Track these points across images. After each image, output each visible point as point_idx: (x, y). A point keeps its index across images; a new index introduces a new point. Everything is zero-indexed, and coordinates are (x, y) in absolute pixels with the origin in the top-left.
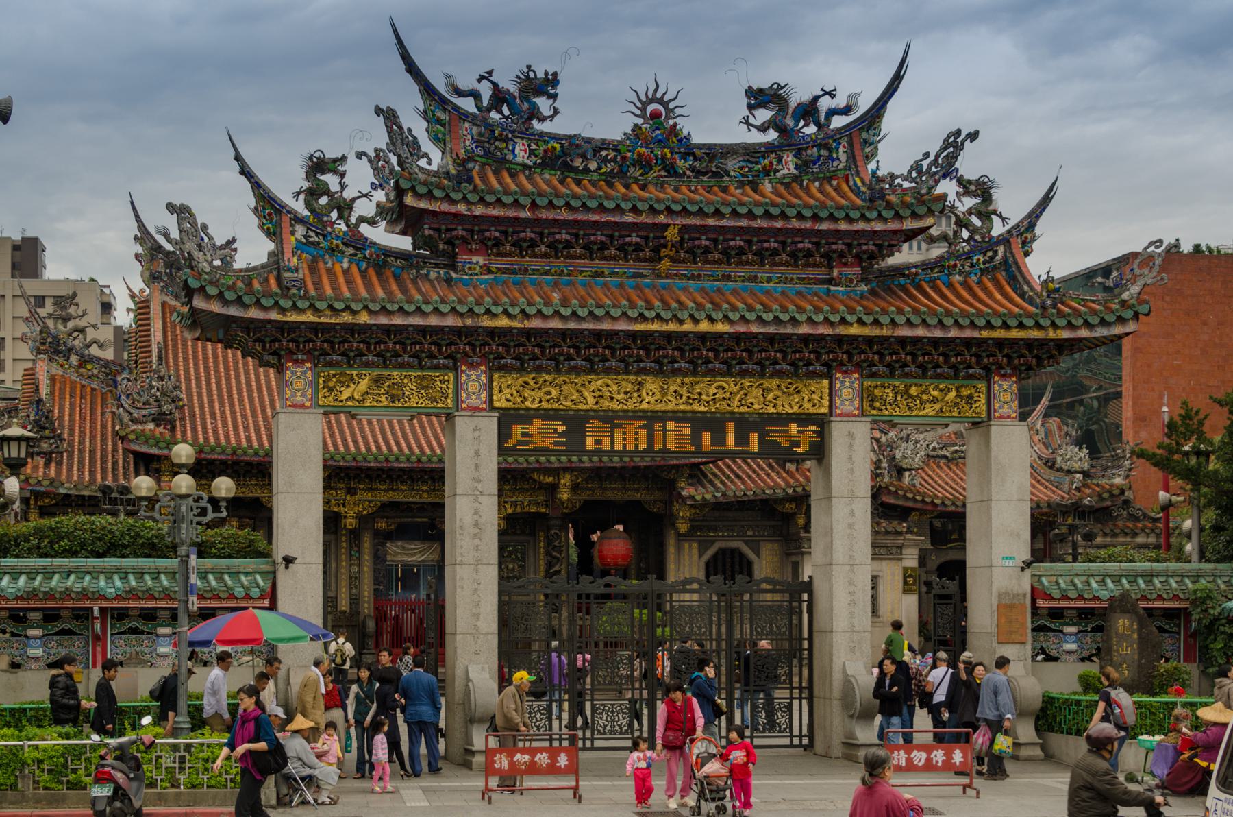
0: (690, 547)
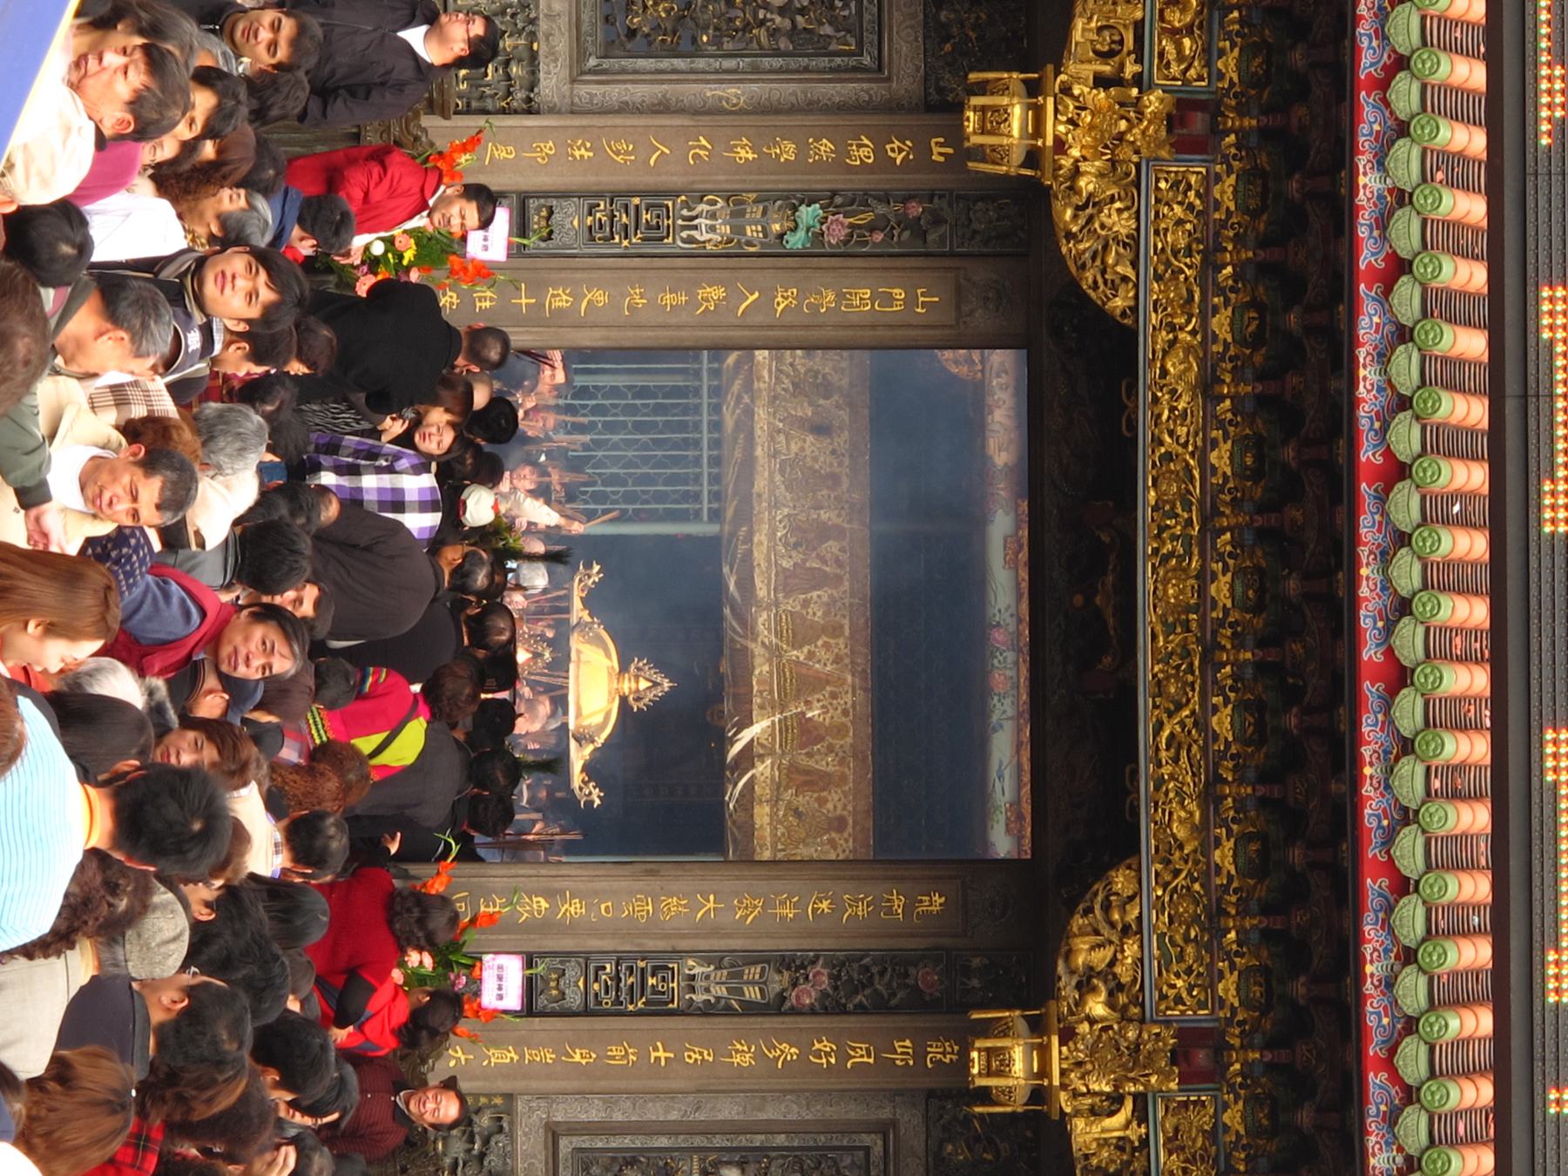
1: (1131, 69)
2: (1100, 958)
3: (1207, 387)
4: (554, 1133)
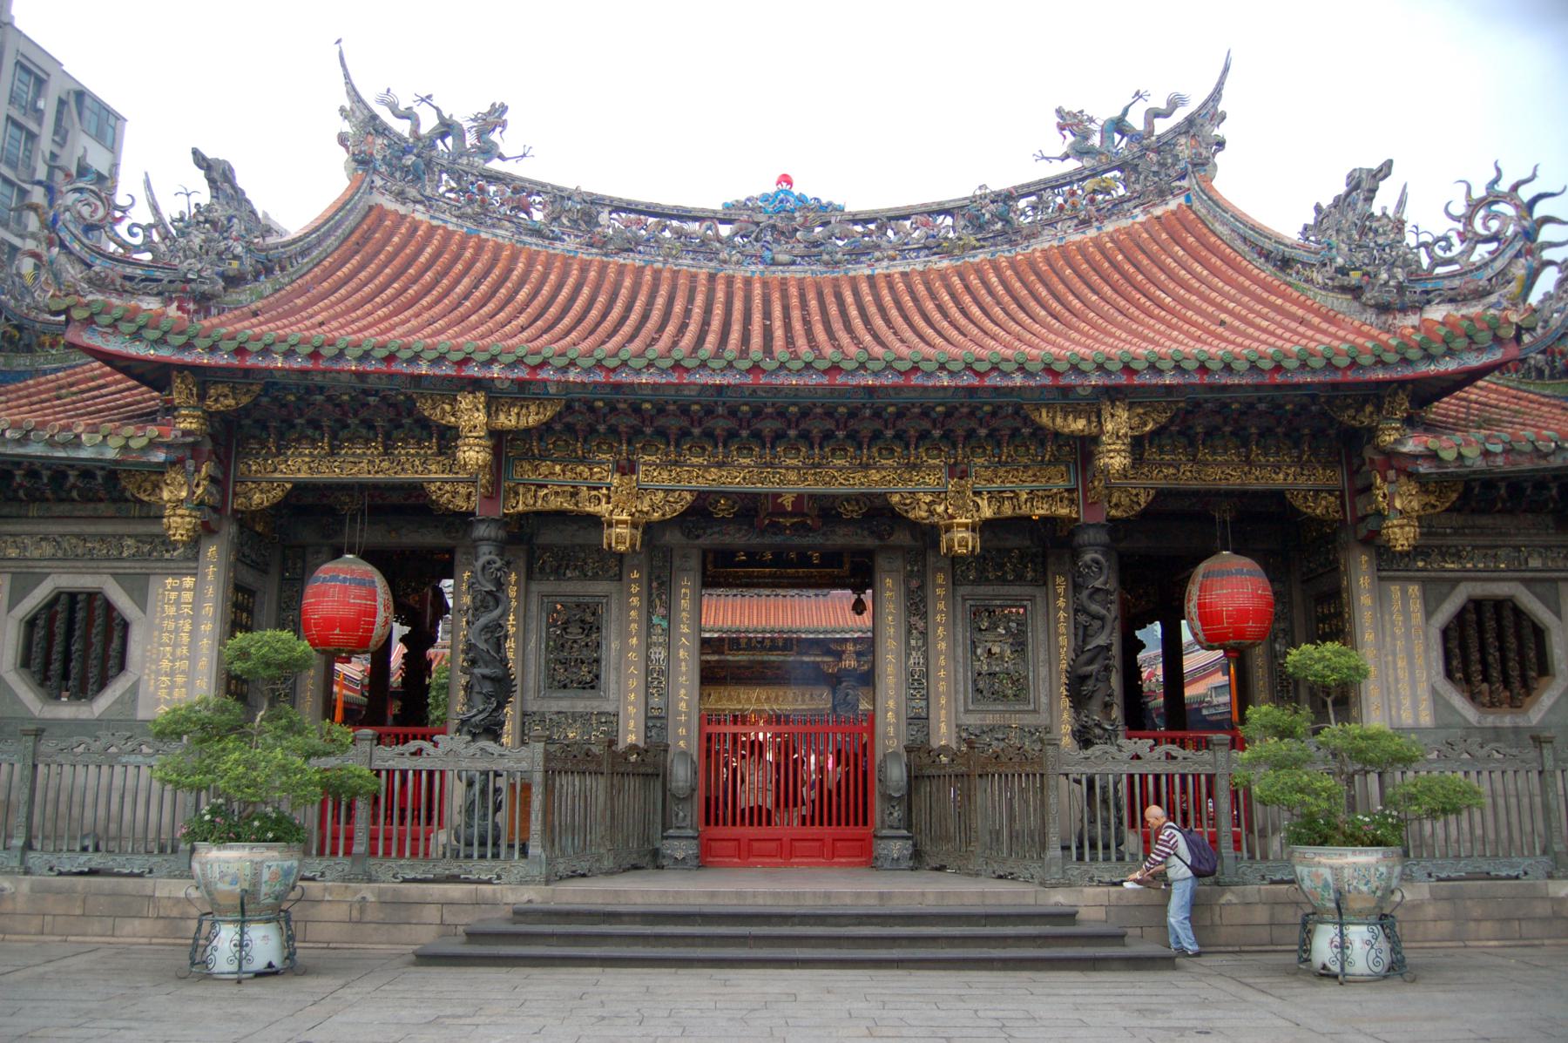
0: (1404, 592)
1: (604, 491)
2: (924, 507)
3: (720, 465)
4: (967, 711)
